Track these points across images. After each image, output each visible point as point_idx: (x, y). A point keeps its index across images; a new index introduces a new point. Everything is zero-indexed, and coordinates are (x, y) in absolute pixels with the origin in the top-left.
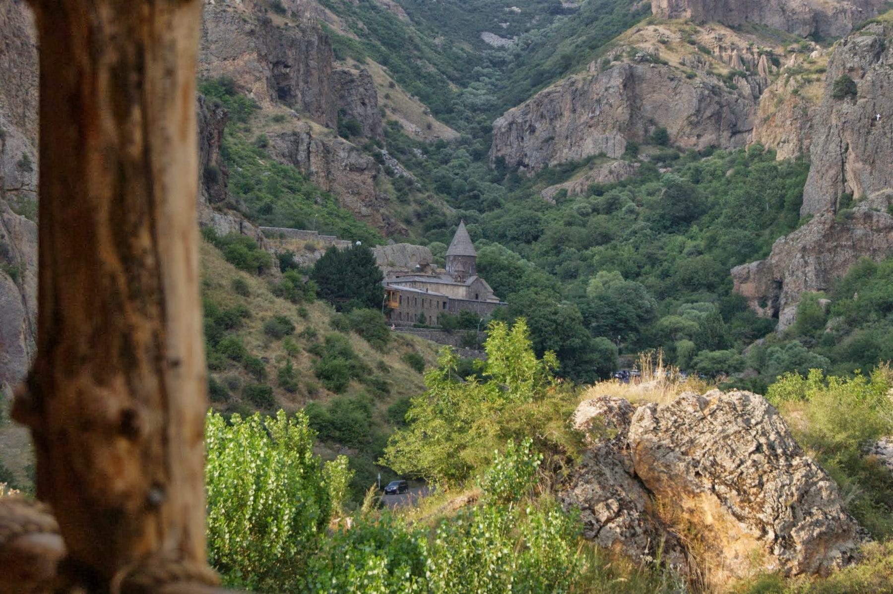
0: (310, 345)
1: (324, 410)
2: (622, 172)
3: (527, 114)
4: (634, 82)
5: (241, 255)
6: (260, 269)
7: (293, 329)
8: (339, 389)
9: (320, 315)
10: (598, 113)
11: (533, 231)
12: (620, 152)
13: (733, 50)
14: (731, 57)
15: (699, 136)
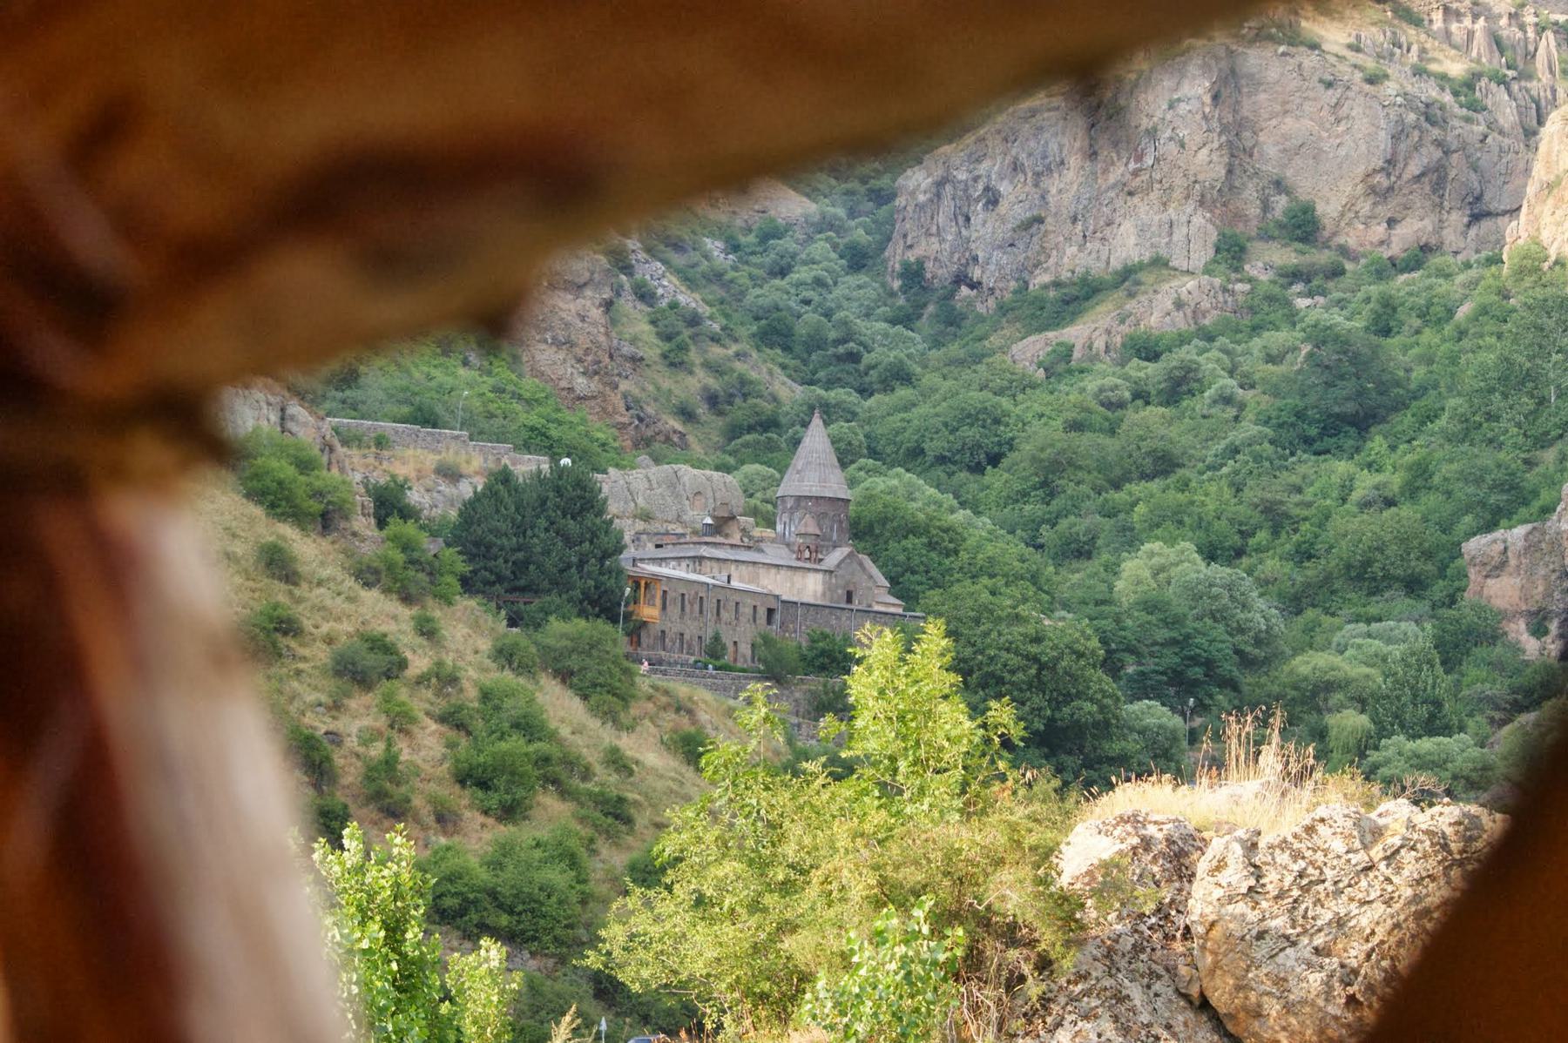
0: (441, 705)
1: (474, 862)
2: (1206, 305)
3: (978, 161)
4: (1238, 89)
5: (280, 483)
6: (327, 520)
7: (403, 664)
8: (510, 812)
9: (469, 635)
10: (1149, 161)
11: (989, 442)
12: (1202, 254)
13: (1475, 17)
14: (1471, 34)
15: (1391, 222)
